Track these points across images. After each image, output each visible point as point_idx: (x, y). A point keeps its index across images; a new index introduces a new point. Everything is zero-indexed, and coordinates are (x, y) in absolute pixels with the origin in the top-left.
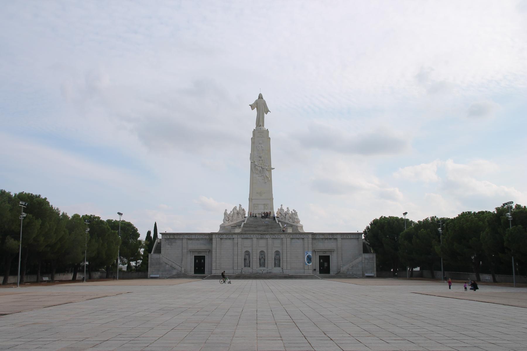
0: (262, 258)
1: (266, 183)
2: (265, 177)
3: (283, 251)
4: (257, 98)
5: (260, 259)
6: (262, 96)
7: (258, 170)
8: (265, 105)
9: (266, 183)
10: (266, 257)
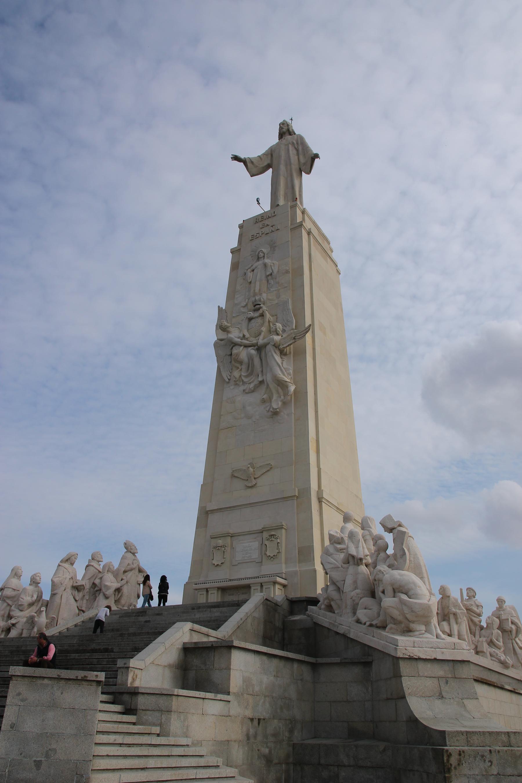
1: (275, 413)
7: (241, 363)
8: (300, 148)
9: (275, 413)
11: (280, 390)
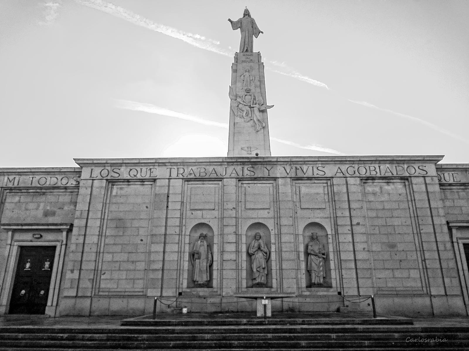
0: (259, 248)
2: (257, 122)
3: (336, 225)
4: (242, 16)
5: (250, 255)
6: (249, 12)
10: (273, 249)
11: (260, 124)
